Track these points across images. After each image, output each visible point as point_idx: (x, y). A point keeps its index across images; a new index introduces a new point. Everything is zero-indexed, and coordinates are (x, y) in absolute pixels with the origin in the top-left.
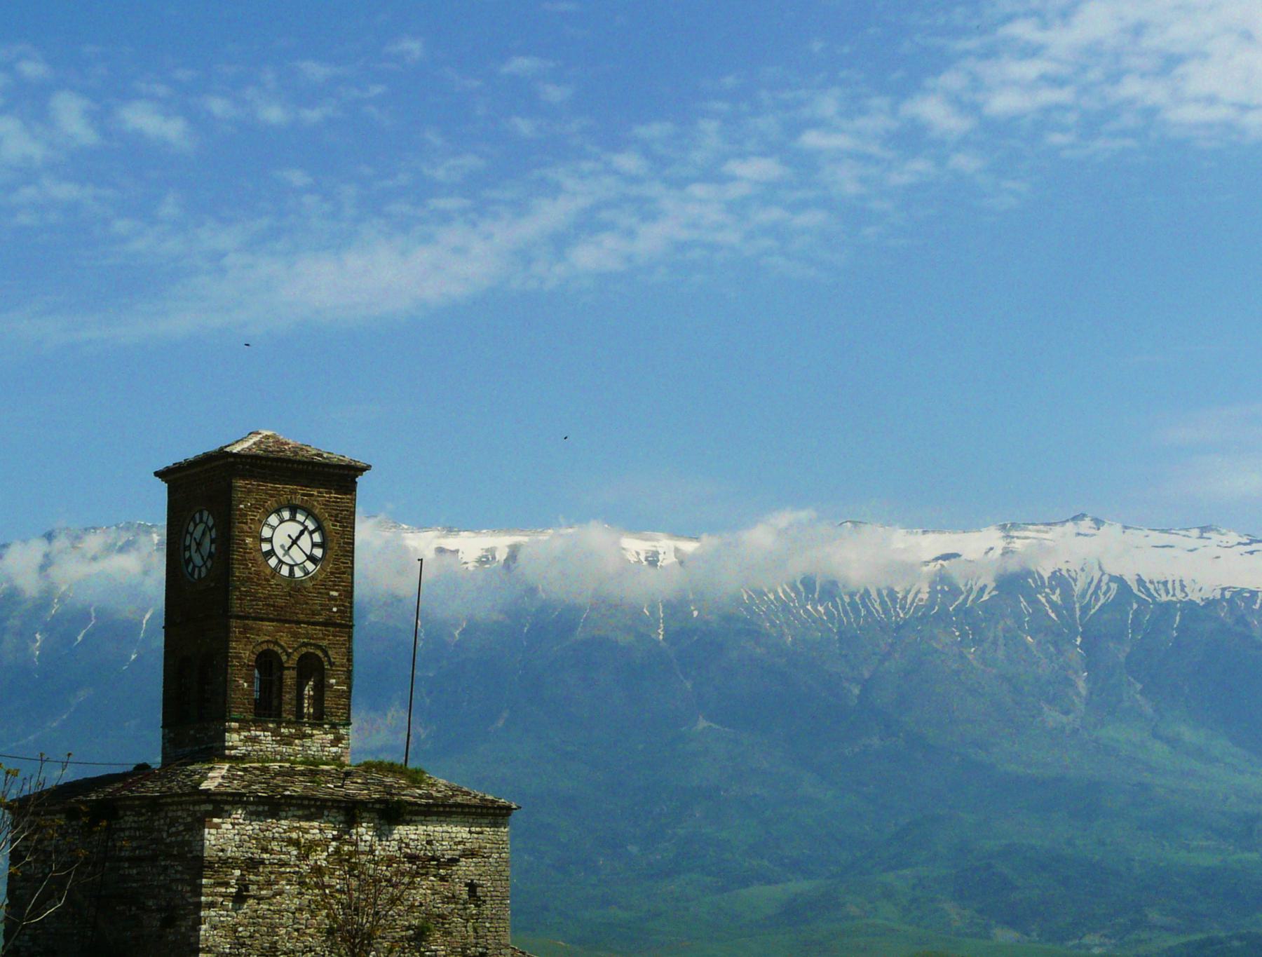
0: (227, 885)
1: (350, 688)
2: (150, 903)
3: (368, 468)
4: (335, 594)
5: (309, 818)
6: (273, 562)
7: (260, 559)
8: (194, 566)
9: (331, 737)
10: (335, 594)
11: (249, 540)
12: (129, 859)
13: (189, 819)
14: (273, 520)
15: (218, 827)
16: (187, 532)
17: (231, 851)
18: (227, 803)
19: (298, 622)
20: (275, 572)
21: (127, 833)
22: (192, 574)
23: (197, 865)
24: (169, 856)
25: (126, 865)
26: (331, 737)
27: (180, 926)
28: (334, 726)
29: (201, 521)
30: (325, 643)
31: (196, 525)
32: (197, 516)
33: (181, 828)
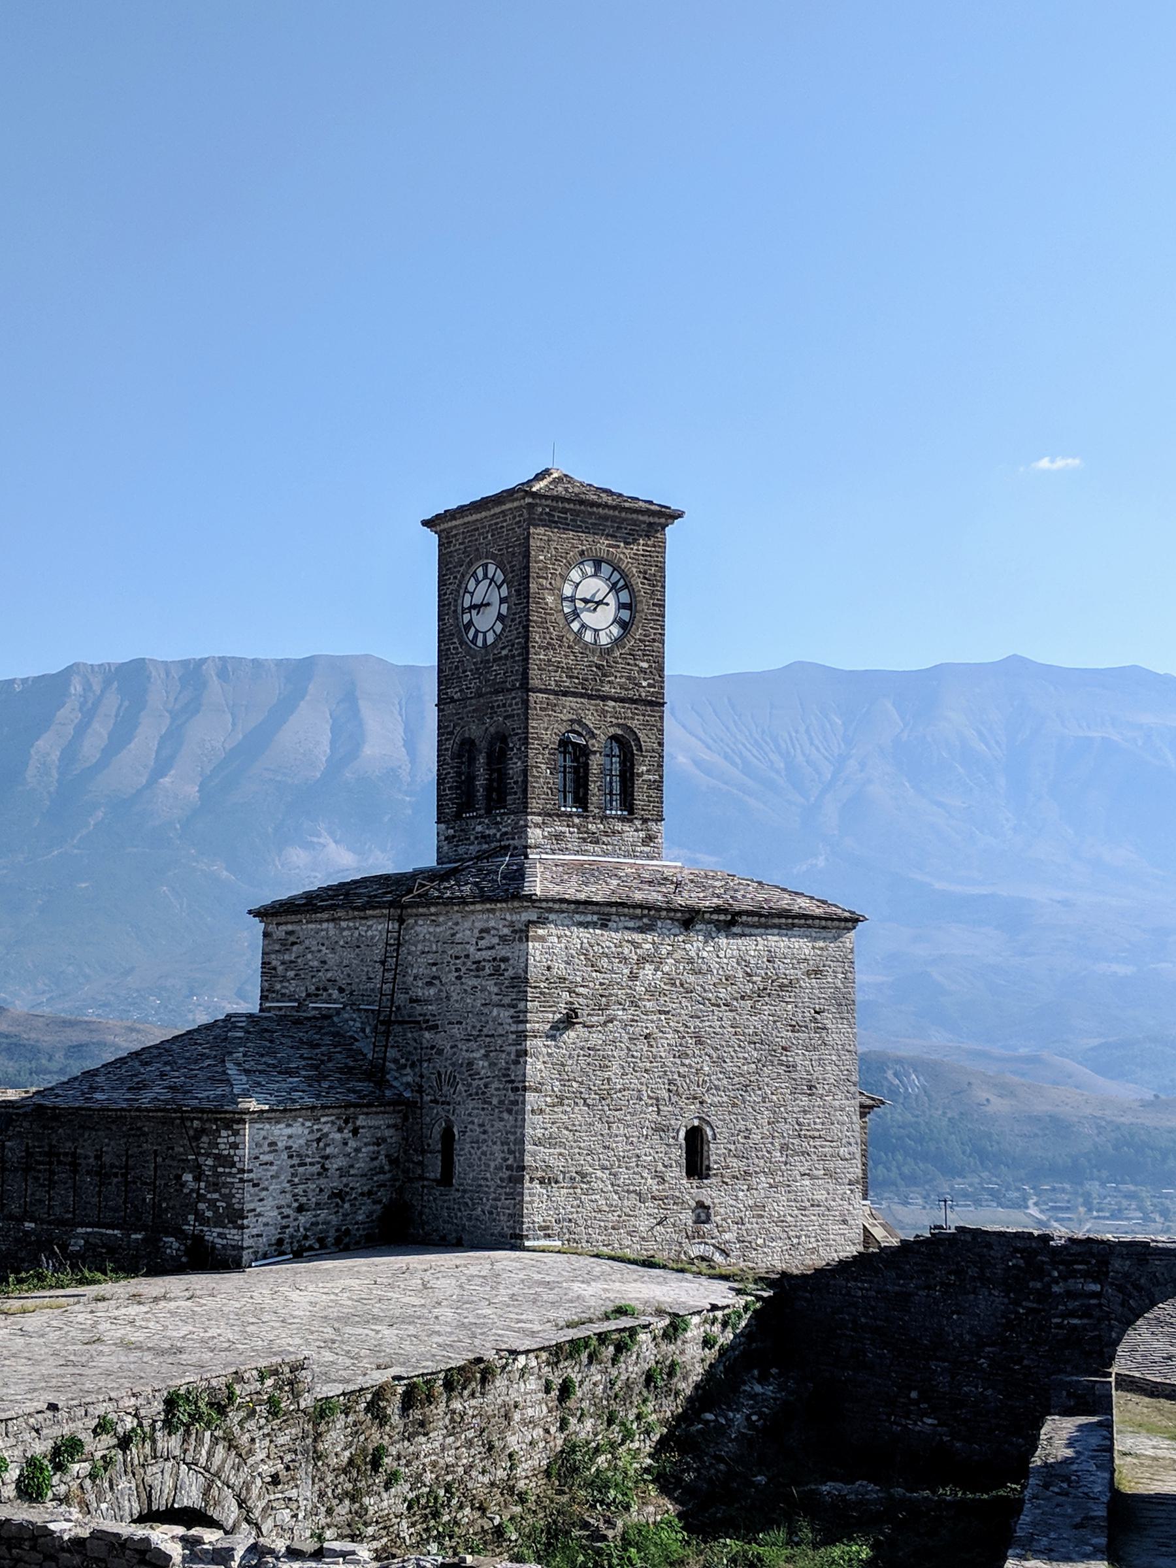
1: (661, 777)
3: (676, 515)
4: (645, 665)
5: (641, 930)
6: (575, 626)
7: (562, 622)
8: (477, 631)
9: (642, 834)
10: (645, 665)
11: (550, 599)
13: (506, 931)
14: (575, 575)
15: (542, 939)
16: (466, 591)
17: (559, 968)
18: (550, 910)
19: (604, 698)
20: (578, 635)
26: (642, 834)
28: (645, 821)
29: (485, 576)
31: (478, 582)
32: (480, 573)
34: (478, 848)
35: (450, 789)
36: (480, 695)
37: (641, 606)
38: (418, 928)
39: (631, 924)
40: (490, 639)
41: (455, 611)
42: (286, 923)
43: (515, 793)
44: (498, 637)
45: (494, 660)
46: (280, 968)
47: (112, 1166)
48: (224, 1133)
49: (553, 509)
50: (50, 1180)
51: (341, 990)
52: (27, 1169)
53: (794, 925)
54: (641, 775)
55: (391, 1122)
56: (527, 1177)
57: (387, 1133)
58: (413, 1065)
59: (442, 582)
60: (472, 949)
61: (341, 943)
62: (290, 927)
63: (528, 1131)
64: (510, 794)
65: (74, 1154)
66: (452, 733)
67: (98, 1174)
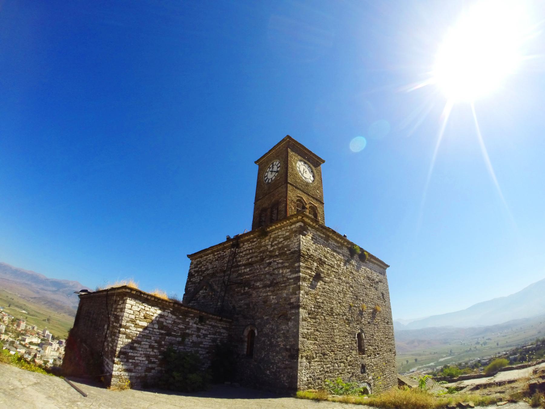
0: (311, 269)
2: (258, 284)
12: (244, 265)
21: (244, 253)
23: (298, 255)
24: (271, 257)
25: (243, 267)
27: (281, 294)
33: (282, 239)
39: (336, 244)
53: (375, 263)
55: (224, 326)
56: (300, 356)
57: (222, 331)
59: (259, 174)
60: (269, 247)
63: (301, 330)
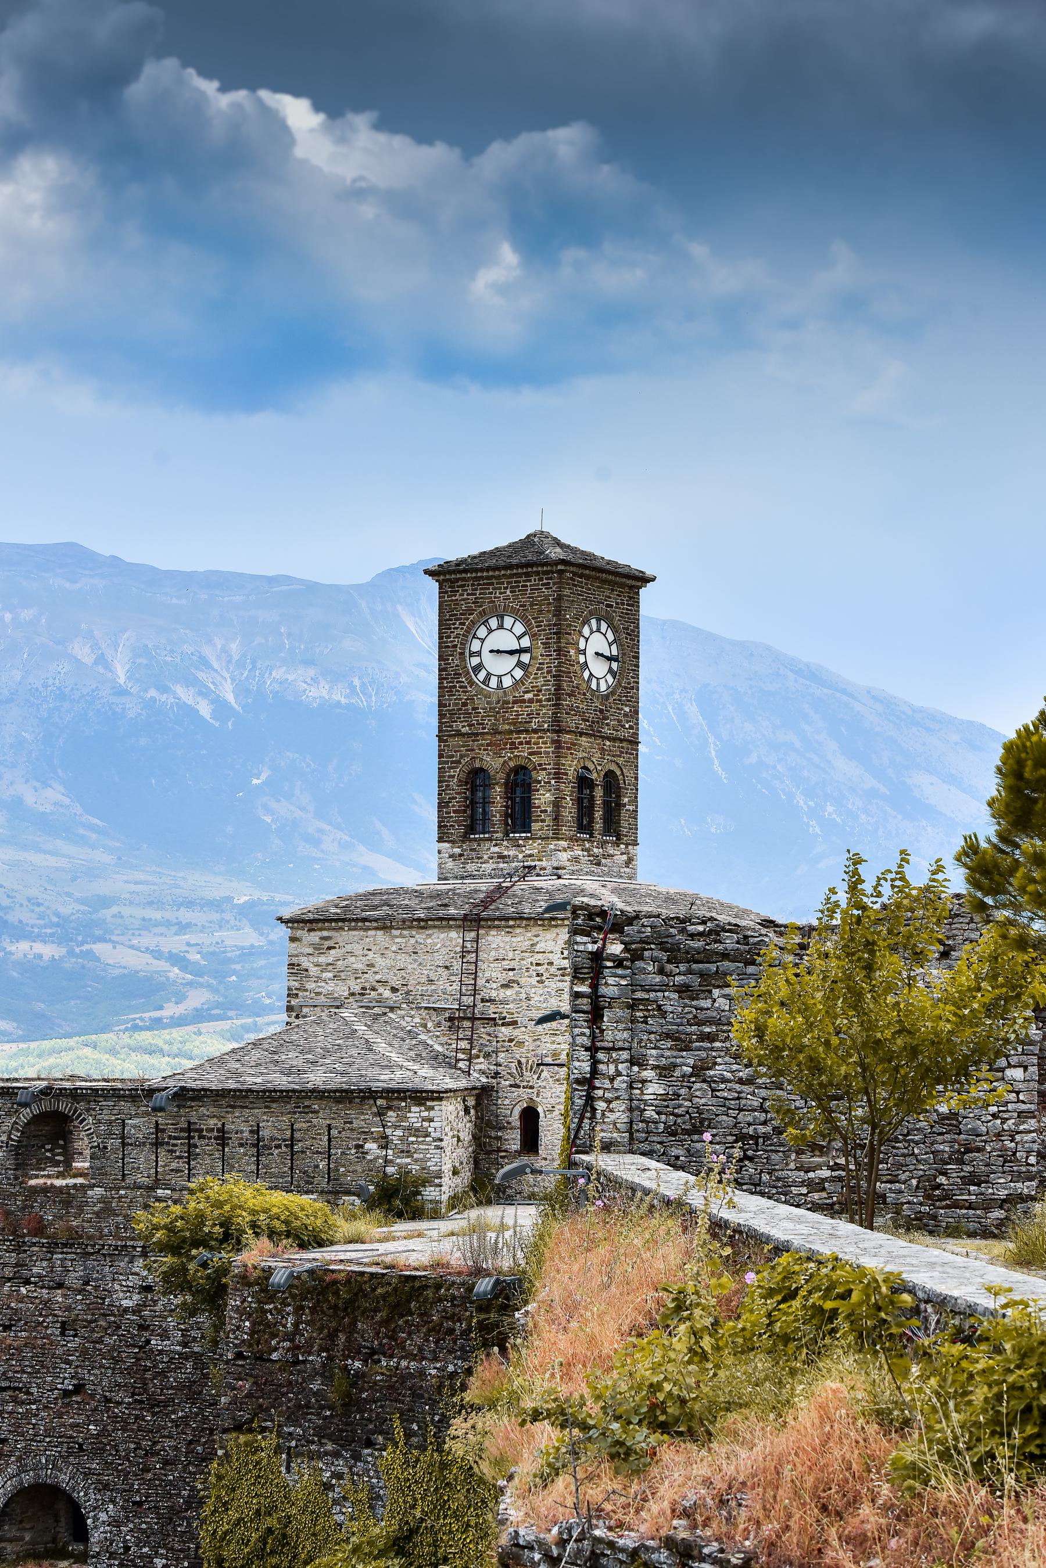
1: (637, 807)
4: (627, 709)
9: (625, 857)
22: (486, 681)
26: (625, 857)
28: (627, 845)
30: (620, 761)
34: (494, 866)
35: (455, 812)
36: (497, 732)
37: (626, 659)
38: (490, 938)
40: (507, 682)
41: (462, 654)
42: (321, 930)
43: (543, 821)
44: (517, 683)
45: (515, 702)
46: (313, 971)
47: (272, 1139)
48: (414, 1109)
49: (575, 574)
50: (189, 1152)
51: (394, 990)
52: (157, 1144)
54: (625, 805)
58: (487, 1056)
61: (394, 948)
62: (325, 933)
64: (537, 821)
65: (222, 1130)
66: (459, 762)
67: (256, 1146)
